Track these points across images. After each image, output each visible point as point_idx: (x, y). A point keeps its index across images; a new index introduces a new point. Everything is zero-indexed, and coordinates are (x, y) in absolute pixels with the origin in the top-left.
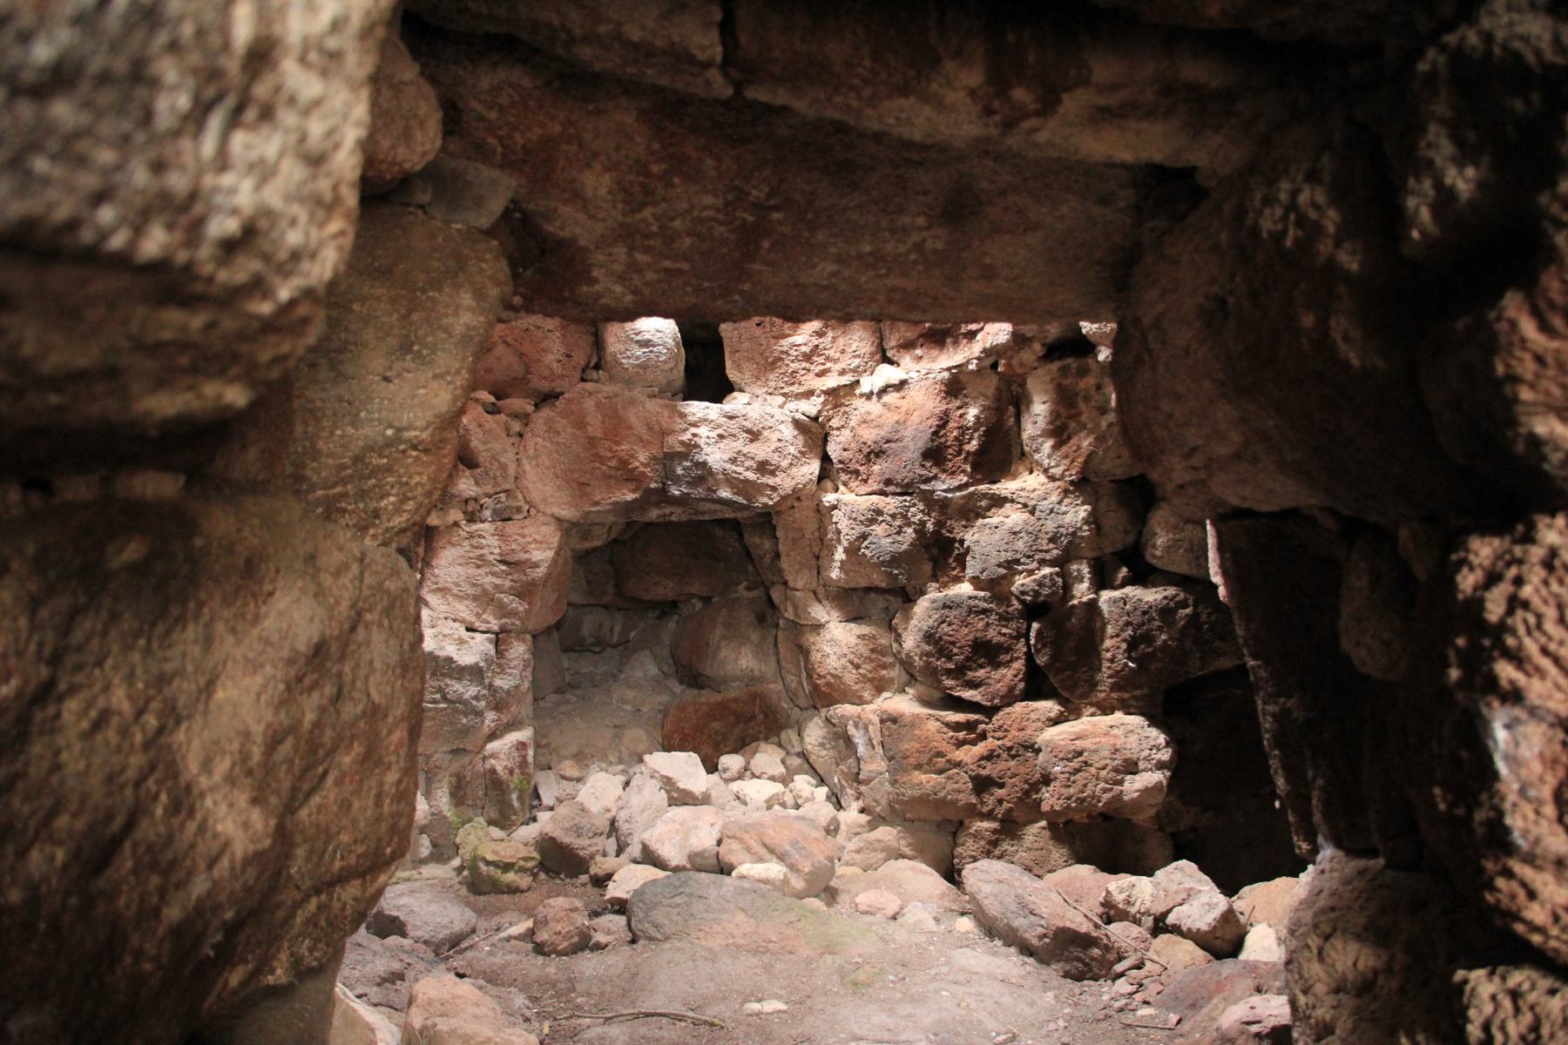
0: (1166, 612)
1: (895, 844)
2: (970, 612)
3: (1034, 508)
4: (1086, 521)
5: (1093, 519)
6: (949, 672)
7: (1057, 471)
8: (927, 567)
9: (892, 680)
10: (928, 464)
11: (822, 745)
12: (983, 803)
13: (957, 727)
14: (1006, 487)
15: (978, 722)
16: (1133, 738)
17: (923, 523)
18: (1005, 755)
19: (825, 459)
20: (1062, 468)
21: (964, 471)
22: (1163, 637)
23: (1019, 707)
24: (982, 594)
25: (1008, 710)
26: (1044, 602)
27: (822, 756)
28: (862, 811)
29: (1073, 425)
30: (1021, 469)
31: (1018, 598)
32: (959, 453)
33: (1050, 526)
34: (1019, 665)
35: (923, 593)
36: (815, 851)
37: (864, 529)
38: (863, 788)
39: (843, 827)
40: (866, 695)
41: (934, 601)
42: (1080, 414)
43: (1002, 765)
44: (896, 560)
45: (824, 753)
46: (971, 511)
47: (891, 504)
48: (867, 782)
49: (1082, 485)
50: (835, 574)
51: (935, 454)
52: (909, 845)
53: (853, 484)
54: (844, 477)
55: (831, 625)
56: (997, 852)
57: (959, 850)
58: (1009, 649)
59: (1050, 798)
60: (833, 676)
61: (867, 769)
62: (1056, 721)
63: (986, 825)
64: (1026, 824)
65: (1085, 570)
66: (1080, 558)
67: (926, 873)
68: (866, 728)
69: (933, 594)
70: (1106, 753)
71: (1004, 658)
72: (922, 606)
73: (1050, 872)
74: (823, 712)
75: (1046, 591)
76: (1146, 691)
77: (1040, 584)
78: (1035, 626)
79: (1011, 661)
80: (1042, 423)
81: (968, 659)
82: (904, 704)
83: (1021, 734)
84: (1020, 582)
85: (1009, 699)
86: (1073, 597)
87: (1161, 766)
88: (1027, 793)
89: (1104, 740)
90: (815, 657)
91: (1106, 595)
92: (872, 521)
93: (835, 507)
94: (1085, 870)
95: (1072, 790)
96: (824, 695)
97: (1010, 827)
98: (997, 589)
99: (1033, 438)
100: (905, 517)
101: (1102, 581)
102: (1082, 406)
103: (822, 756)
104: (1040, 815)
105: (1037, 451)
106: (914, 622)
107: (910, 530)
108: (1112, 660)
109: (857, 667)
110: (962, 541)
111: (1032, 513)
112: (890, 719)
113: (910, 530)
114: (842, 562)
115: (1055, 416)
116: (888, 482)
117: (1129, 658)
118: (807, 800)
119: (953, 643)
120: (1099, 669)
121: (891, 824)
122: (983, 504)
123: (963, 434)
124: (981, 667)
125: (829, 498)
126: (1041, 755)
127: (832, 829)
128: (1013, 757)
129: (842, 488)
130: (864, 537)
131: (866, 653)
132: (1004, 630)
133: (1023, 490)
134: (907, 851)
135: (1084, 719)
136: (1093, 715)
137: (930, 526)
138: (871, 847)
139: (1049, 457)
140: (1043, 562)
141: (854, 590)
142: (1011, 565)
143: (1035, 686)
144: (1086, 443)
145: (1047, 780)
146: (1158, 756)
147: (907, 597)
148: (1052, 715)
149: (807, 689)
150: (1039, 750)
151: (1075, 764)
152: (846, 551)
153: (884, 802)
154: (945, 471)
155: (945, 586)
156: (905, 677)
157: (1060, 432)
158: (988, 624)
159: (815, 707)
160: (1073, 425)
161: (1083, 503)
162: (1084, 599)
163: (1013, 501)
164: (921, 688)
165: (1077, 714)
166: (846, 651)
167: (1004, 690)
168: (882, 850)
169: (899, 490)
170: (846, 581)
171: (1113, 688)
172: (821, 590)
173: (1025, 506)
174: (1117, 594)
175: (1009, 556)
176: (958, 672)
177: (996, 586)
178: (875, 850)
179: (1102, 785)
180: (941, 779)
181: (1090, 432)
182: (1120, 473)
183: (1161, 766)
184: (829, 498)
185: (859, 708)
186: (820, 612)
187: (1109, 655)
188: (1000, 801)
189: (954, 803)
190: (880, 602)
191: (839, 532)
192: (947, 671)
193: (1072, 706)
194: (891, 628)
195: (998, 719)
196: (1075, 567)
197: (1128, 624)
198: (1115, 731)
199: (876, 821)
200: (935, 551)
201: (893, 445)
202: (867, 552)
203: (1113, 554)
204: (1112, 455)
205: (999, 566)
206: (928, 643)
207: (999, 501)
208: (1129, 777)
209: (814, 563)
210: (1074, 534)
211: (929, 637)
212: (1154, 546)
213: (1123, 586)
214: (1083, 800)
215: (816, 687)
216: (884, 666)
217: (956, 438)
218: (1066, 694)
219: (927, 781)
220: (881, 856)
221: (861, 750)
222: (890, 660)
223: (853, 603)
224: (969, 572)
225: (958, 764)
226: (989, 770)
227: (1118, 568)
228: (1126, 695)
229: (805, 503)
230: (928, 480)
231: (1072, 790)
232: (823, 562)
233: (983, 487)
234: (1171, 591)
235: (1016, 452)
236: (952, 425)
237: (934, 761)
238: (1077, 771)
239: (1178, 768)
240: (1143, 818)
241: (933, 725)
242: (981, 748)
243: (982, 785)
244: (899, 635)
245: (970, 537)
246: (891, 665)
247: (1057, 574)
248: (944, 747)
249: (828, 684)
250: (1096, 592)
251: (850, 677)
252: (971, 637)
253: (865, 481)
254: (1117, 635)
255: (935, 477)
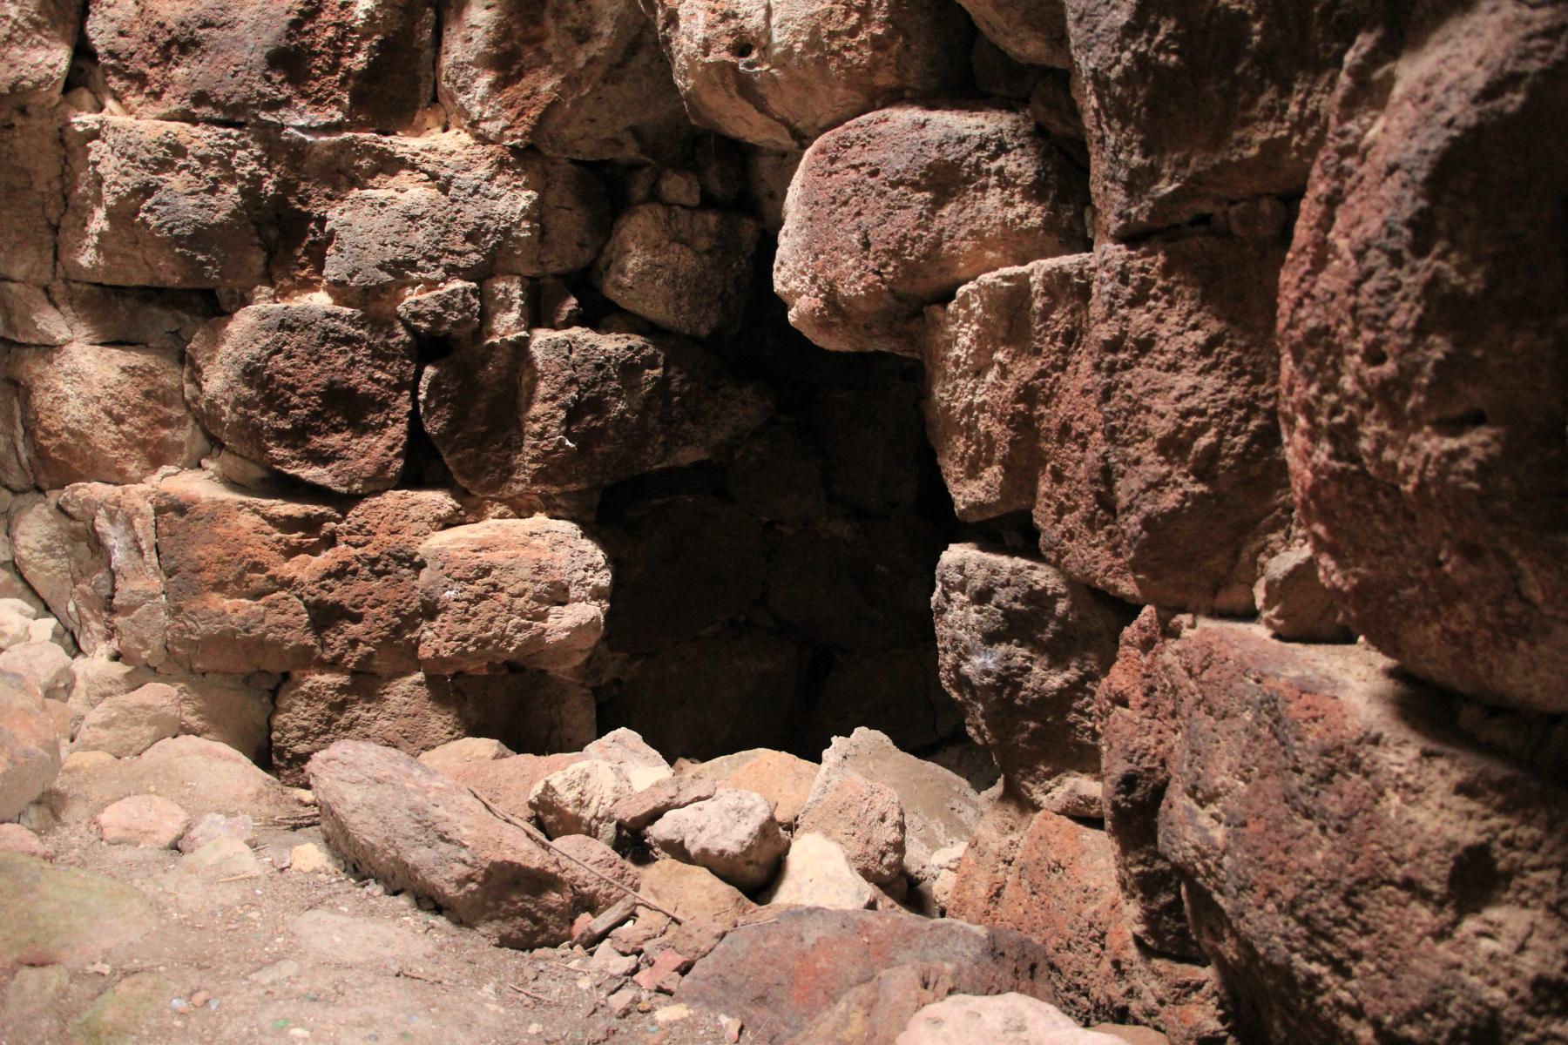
0: (629, 369)
1: (173, 711)
2: (325, 338)
3: (449, 180)
4: (527, 215)
5: (536, 214)
6: (280, 436)
7: (492, 128)
8: (257, 259)
9: (181, 445)
10: (277, 78)
11: (49, 550)
12: (324, 645)
13: (288, 524)
14: (404, 144)
15: (323, 518)
16: (563, 552)
17: (256, 180)
18: (366, 571)
19: (83, 51)
20: (501, 123)
21: (338, 102)
22: (621, 406)
23: (391, 498)
24: (348, 311)
25: (374, 501)
26: (448, 334)
27: (48, 571)
28: (116, 657)
29: (529, 54)
30: (430, 121)
31: (406, 324)
32: (333, 68)
33: (471, 213)
34: (397, 431)
35: (245, 302)
36: (21, 733)
37: (147, 176)
38: (119, 620)
39: (81, 684)
40: (132, 468)
41: (265, 316)
42: (541, 39)
43: (359, 587)
44: (202, 236)
45: (52, 562)
46: (343, 174)
47: (201, 138)
48: (127, 610)
49: (526, 158)
50: (87, 258)
51: (291, 61)
52: (197, 711)
53: (133, 100)
54: (115, 83)
55: (75, 348)
56: (343, 721)
57: (282, 718)
58: (383, 405)
59: (433, 639)
60: (72, 433)
61: (127, 589)
62: (447, 523)
63: (327, 679)
64: (391, 679)
65: (517, 292)
66: (510, 273)
67: (228, 758)
68: (129, 522)
69: (264, 303)
70: (526, 573)
71: (375, 418)
72: (243, 322)
73: (426, 748)
74: (54, 497)
75: (454, 317)
76: (584, 485)
77: (446, 305)
78: (430, 371)
79: (384, 425)
80: (480, 41)
81: (315, 415)
82: (199, 485)
83: (393, 539)
84: (411, 296)
85: (378, 483)
86: (491, 333)
87: (597, 594)
88: (397, 631)
89: (523, 552)
90: (42, 400)
91: (541, 335)
92: (164, 165)
93: (95, 135)
94: (486, 747)
95: (470, 627)
96: (52, 466)
97: (366, 682)
98: (373, 307)
99: (460, 66)
100: (225, 164)
101: (537, 315)
102: (550, 23)
103: (48, 571)
104: (419, 665)
105: (464, 89)
106: (226, 348)
107: (233, 190)
108: (540, 436)
109: (119, 420)
110: (322, 221)
111: (444, 189)
112: (174, 509)
113: (233, 190)
114: (101, 235)
115: (503, 33)
116: (201, 98)
117: (567, 434)
118: (16, 639)
119: (293, 388)
120: (519, 449)
121: (168, 679)
122: (364, 163)
123: (343, 38)
124: (336, 429)
125: (84, 119)
126: (424, 573)
127: (59, 689)
128: (379, 575)
129: (110, 104)
130: (147, 190)
131: (137, 399)
132: (378, 374)
133: (432, 150)
134: (194, 721)
135: (490, 522)
136: (502, 516)
137: (269, 186)
138: (131, 717)
139: (482, 102)
140: (452, 271)
141: (119, 290)
142: (400, 269)
143: (420, 466)
144: (548, 86)
145: (430, 610)
146: (595, 580)
147: (214, 307)
148: (442, 512)
149: (24, 456)
150: (422, 565)
151: (478, 588)
152: (110, 216)
153: (156, 643)
154: (305, 96)
155: (285, 294)
156: (201, 443)
157: (506, 62)
158: (353, 362)
159: (40, 490)
160: (529, 54)
161: (526, 186)
162: (510, 338)
163: (413, 167)
164: (230, 460)
165: (480, 517)
166: (98, 392)
167: (371, 469)
168: (151, 723)
169: (218, 115)
170: (108, 272)
171: (540, 477)
172: (59, 288)
173: (433, 177)
174: (561, 335)
175: (400, 253)
176: (296, 437)
177: (371, 301)
178: (137, 722)
179: (517, 620)
180: (258, 606)
181: (558, 69)
182: (586, 151)
183: (597, 594)
184: (84, 119)
185: (118, 490)
186: (53, 323)
187: (537, 427)
188: (354, 643)
189: (278, 644)
190: (164, 320)
191: (99, 180)
192: (272, 437)
193: (474, 502)
194: (182, 358)
195: (356, 515)
196: (501, 285)
197: (572, 381)
198: (537, 541)
199: (141, 672)
200: (273, 233)
201: (216, 33)
202: (150, 218)
203: (556, 276)
204: (583, 113)
205: (382, 267)
206: (250, 385)
207: (390, 164)
208: (554, 609)
209: (48, 237)
210: (507, 231)
211: (252, 374)
212: (622, 271)
213: (567, 325)
214: (487, 642)
215: (41, 453)
216: (166, 423)
217: (331, 42)
218: (464, 483)
219: (233, 608)
220: (149, 731)
221: (119, 558)
222: (177, 412)
223: (119, 310)
224: (330, 272)
225: (288, 584)
226: (339, 593)
227: (562, 299)
228: (555, 490)
229: (36, 122)
230: (273, 105)
231: (470, 627)
232: (67, 236)
233: (366, 136)
234: (637, 341)
235: (425, 91)
236: (325, 16)
237: (247, 577)
238: (481, 597)
239: (615, 595)
240: (563, 670)
241: (247, 521)
242: (326, 559)
243: (325, 616)
244: (199, 370)
245: (335, 216)
246: (180, 422)
247: (474, 292)
248: (265, 555)
249: (63, 448)
250: (528, 329)
251: (105, 437)
252: (323, 380)
253: (157, 96)
254: (554, 398)
255: (287, 103)
